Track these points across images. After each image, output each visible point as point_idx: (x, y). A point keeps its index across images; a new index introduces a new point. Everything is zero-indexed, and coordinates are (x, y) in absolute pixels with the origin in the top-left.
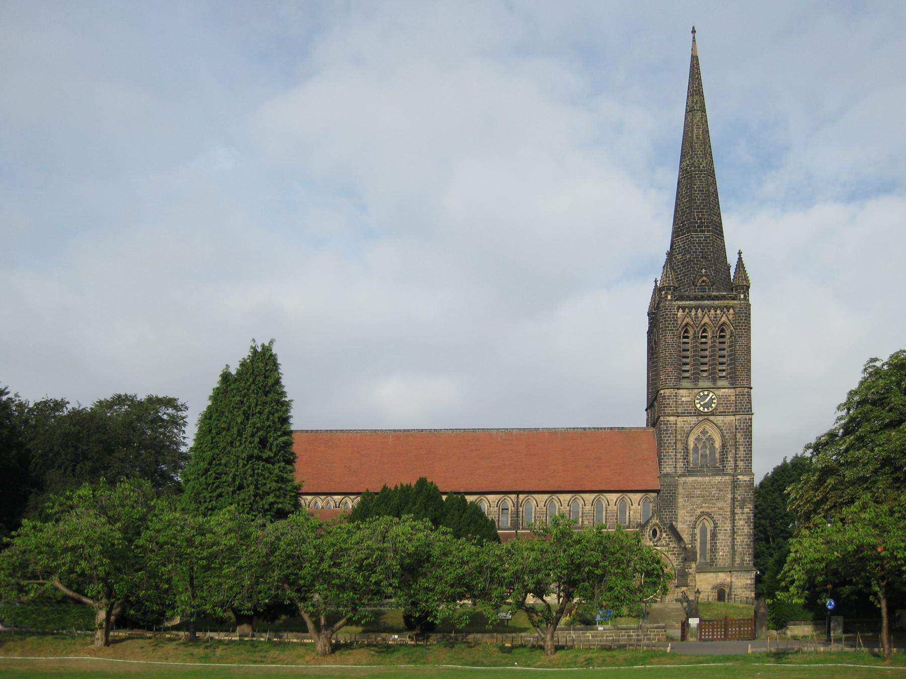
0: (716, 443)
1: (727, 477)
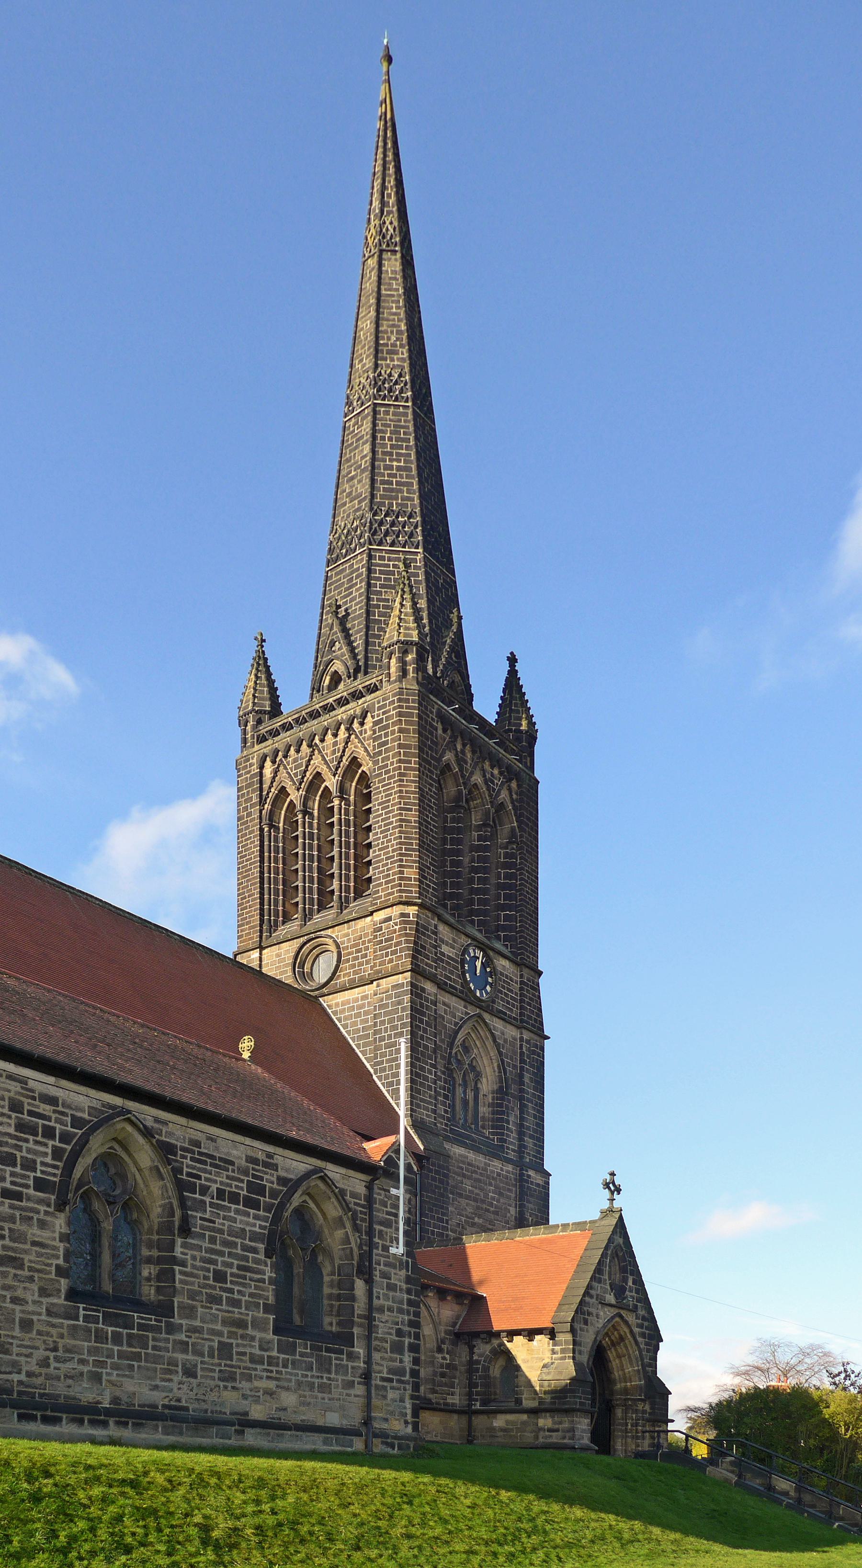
0: (484, 1080)
1: (510, 1168)
